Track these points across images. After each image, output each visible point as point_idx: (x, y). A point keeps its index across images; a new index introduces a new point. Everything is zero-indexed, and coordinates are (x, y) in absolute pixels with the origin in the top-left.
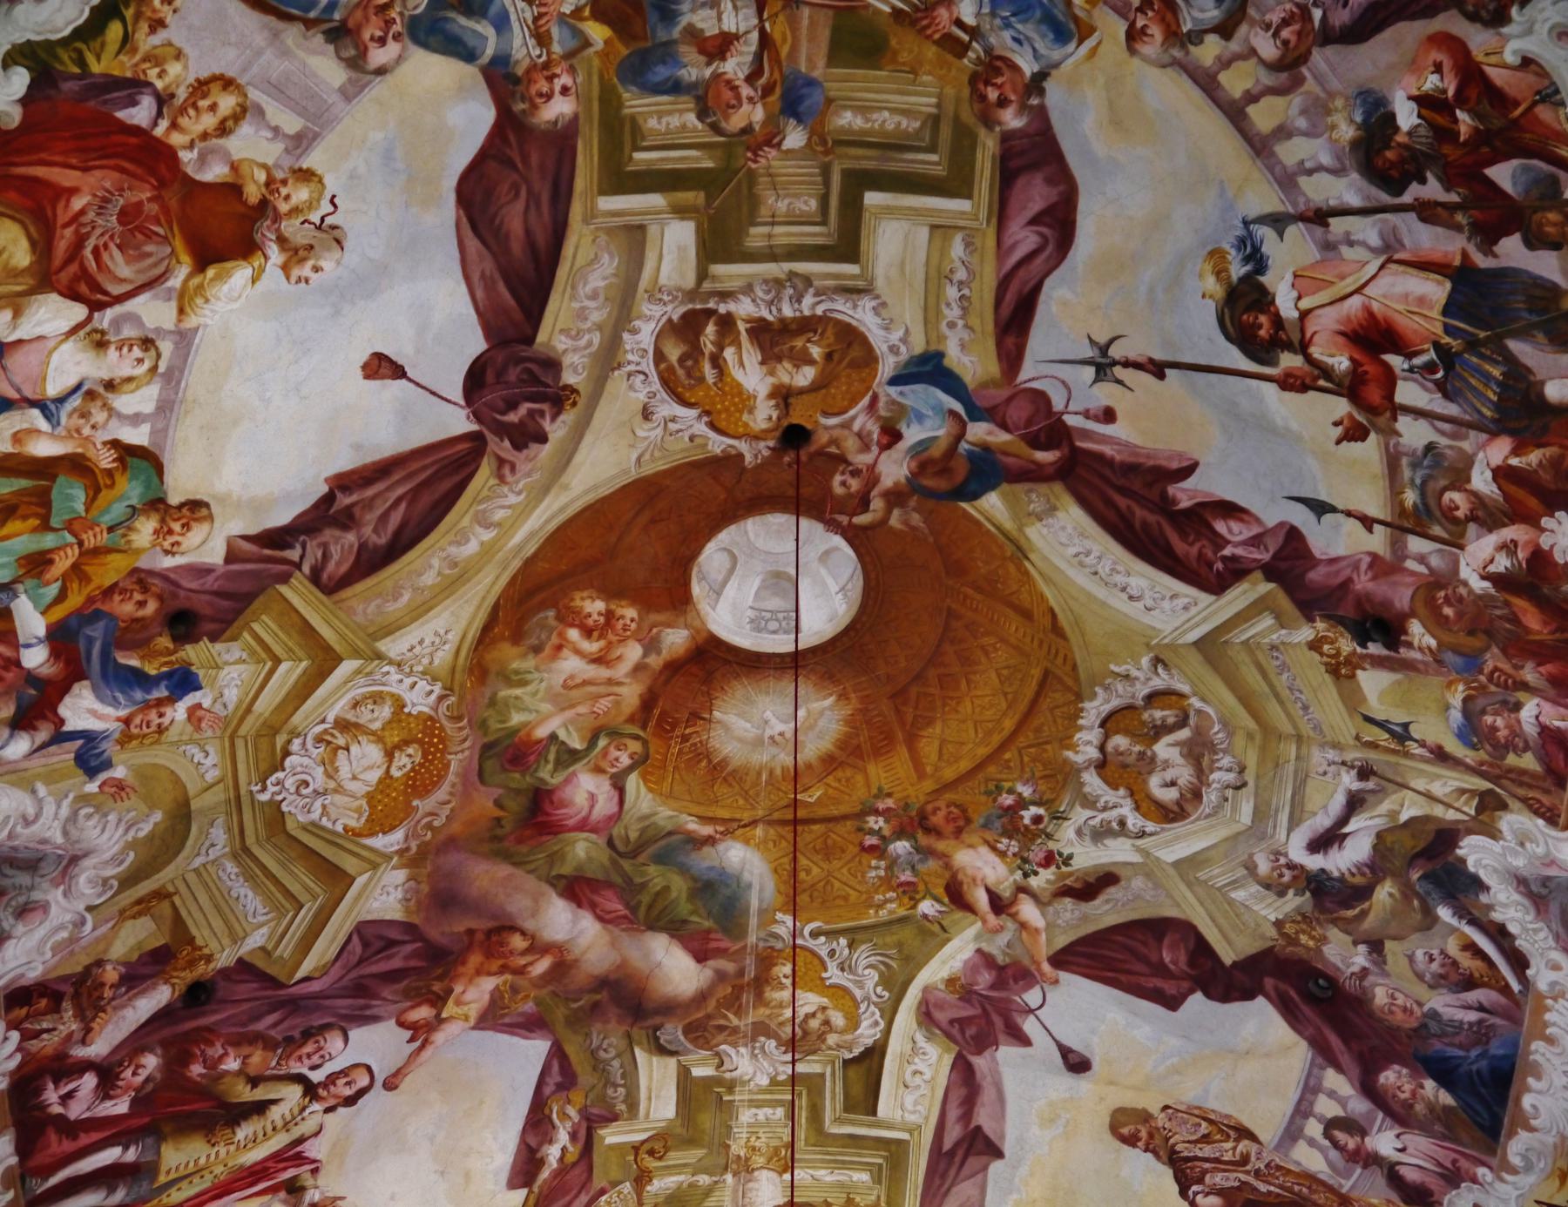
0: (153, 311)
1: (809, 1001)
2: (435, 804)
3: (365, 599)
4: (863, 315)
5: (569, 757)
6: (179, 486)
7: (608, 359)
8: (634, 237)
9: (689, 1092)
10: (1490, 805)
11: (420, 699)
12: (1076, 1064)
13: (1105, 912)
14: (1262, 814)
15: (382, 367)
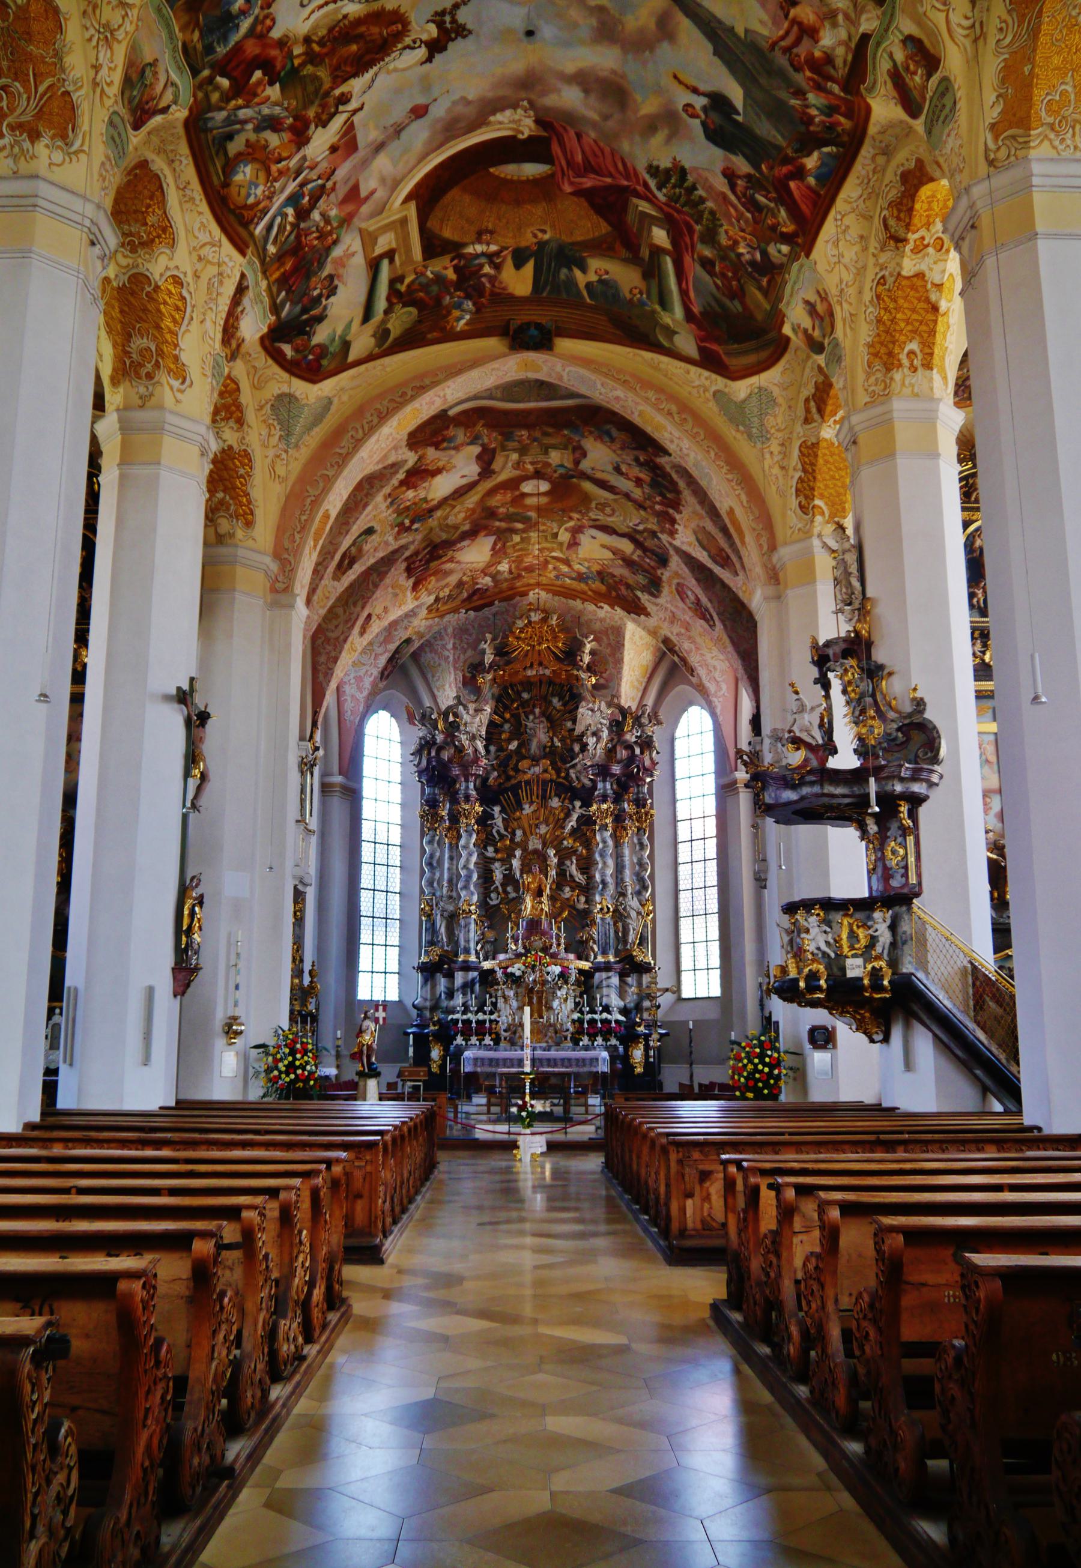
0: (425, 485)
1: (542, 528)
2: (475, 516)
3: (461, 500)
4: (550, 460)
5: (498, 507)
6: (429, 498)
7: (503, 467)
8: (508, 456)
9: (522, 538)
10: (662, 532)
11: (471, 506)
12: (594, 538)
13: (597, 523)
14: (625, 520)
15: (463, 477)
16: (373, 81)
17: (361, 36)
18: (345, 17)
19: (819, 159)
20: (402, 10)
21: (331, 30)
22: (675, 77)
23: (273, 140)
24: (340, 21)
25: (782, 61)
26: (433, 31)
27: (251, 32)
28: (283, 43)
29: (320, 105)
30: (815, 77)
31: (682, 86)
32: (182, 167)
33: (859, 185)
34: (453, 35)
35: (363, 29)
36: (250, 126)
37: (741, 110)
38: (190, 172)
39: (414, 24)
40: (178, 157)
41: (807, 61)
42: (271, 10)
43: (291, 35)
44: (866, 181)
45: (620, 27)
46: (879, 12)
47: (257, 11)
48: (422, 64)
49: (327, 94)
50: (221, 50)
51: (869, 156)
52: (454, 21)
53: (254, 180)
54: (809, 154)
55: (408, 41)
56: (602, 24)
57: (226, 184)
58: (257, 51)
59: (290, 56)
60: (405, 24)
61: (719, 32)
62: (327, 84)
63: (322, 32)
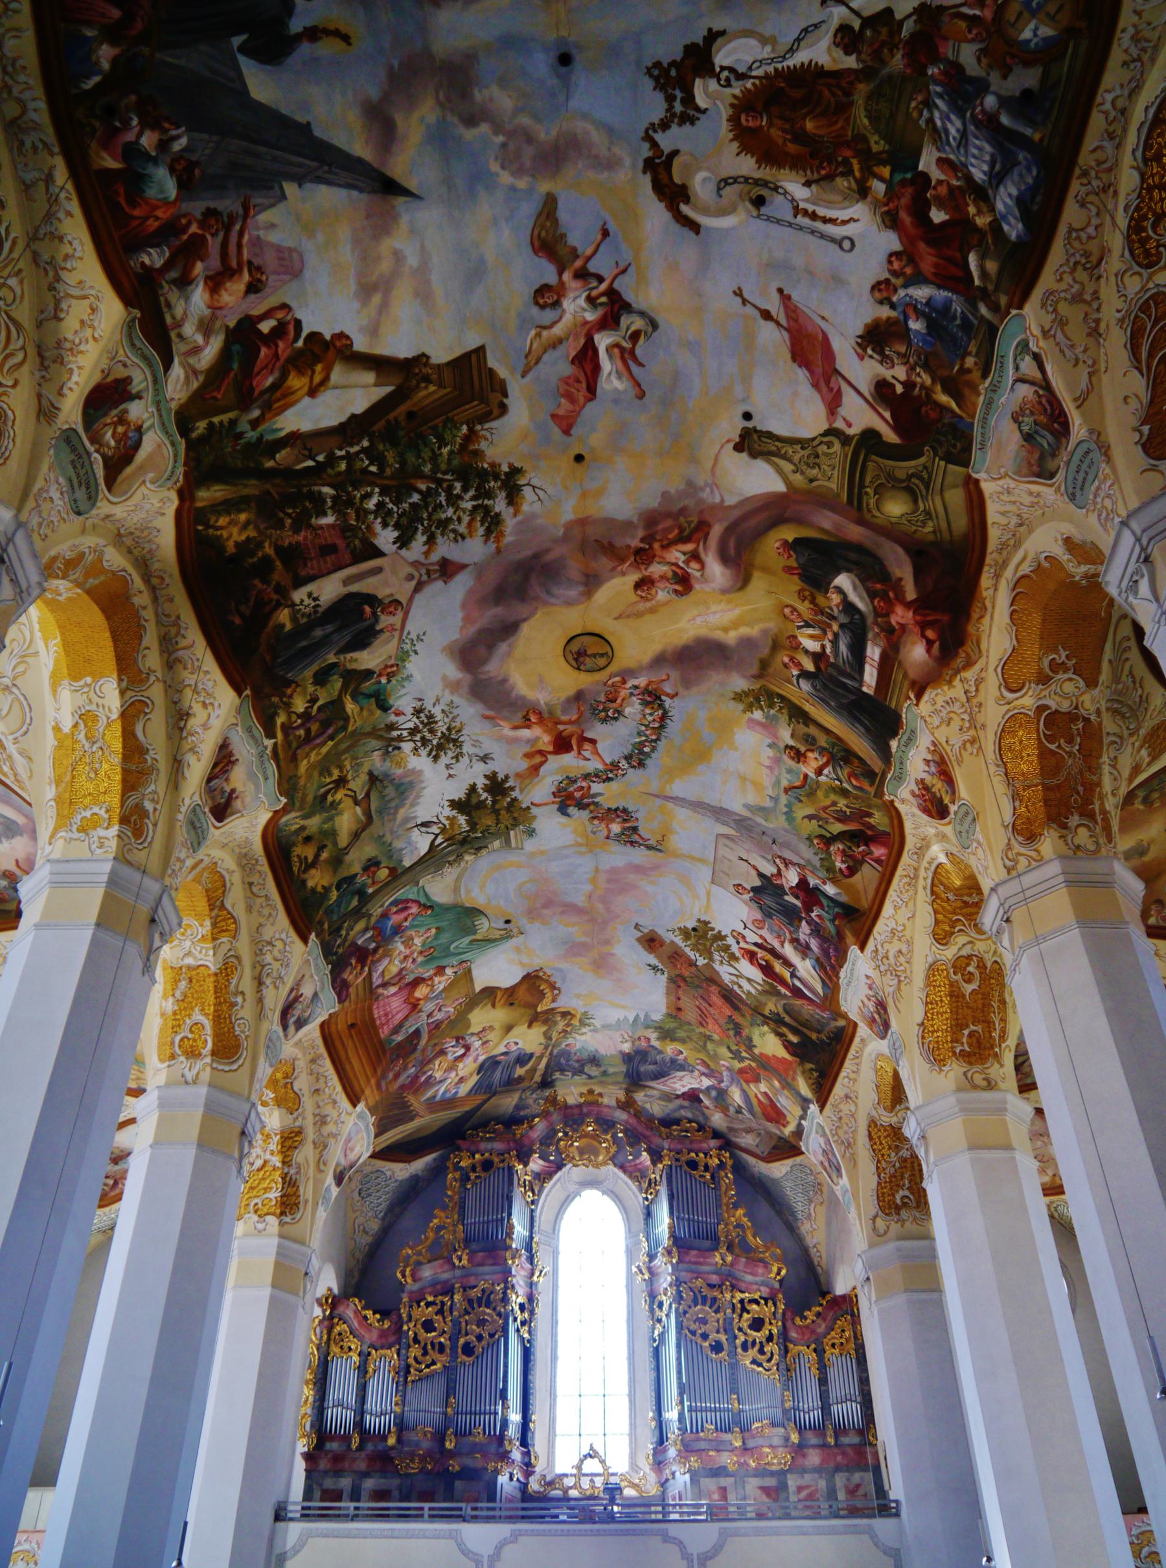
16: (798, 40)
17: (800, 137)
18: (808, 184)
19: (97, 63)
20: (735, 145)
21: (830, 177)
22: (346, 38)
23: (968, 55)
24: (817, 181)
25: (228, 204)
26: (704, 91)
27: (917, 279)
28: (891, 221)
29: (884, 63)
30: (185, 237)
31: (332, 27)
32: (1118, 92)
33: (14, 60)
34: (673, 73)
35: (791, 148)
36: (990, 101)
37: (242, 60)
38: (1113, 77)
39: (725, 116)
40: (1113, 113)
41: (203, 237)
42: (887, 275)
43: (879, 219)
44: (10, 69)
45: (441, 95)
46: (174, 405)
47: (902, 293)
48: (723, 33)
49: (865, 74)
50: (958, 306)
51: (31, 105)
52: (670, 99)
53: (1026, 15)
54: (114, 61)
55: (736, 89)
56: (466, 95)
57: (1069, 32)
58: (922, 246)
59: (890, 194)
60: (734, 120)
61: (314, 164)
62: (863, 89)
63: (842, 183)
